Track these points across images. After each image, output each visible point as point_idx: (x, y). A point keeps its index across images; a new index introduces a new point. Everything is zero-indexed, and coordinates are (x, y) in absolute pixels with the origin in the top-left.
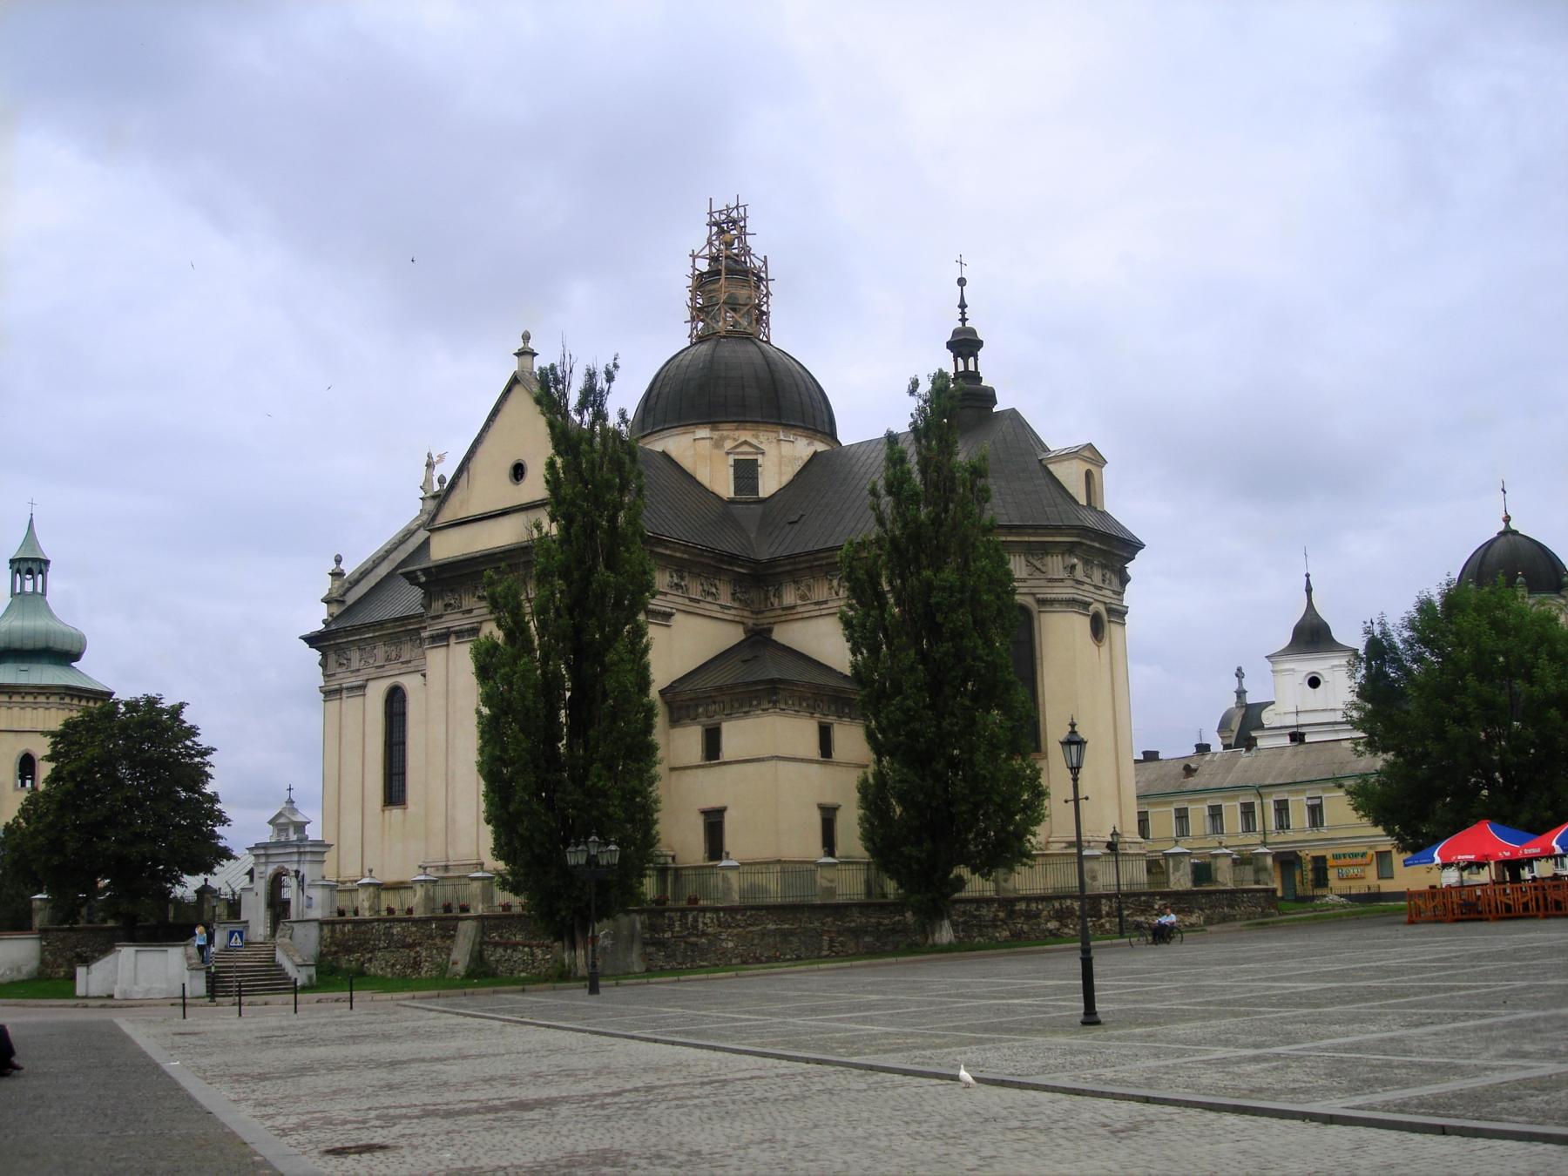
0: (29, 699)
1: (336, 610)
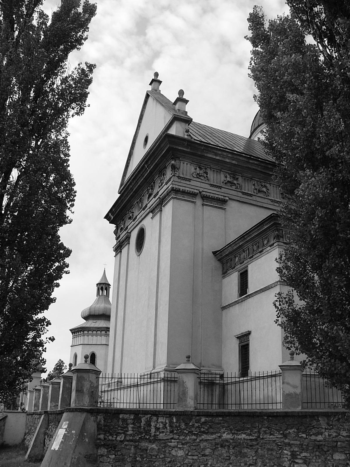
0: (94, 332)
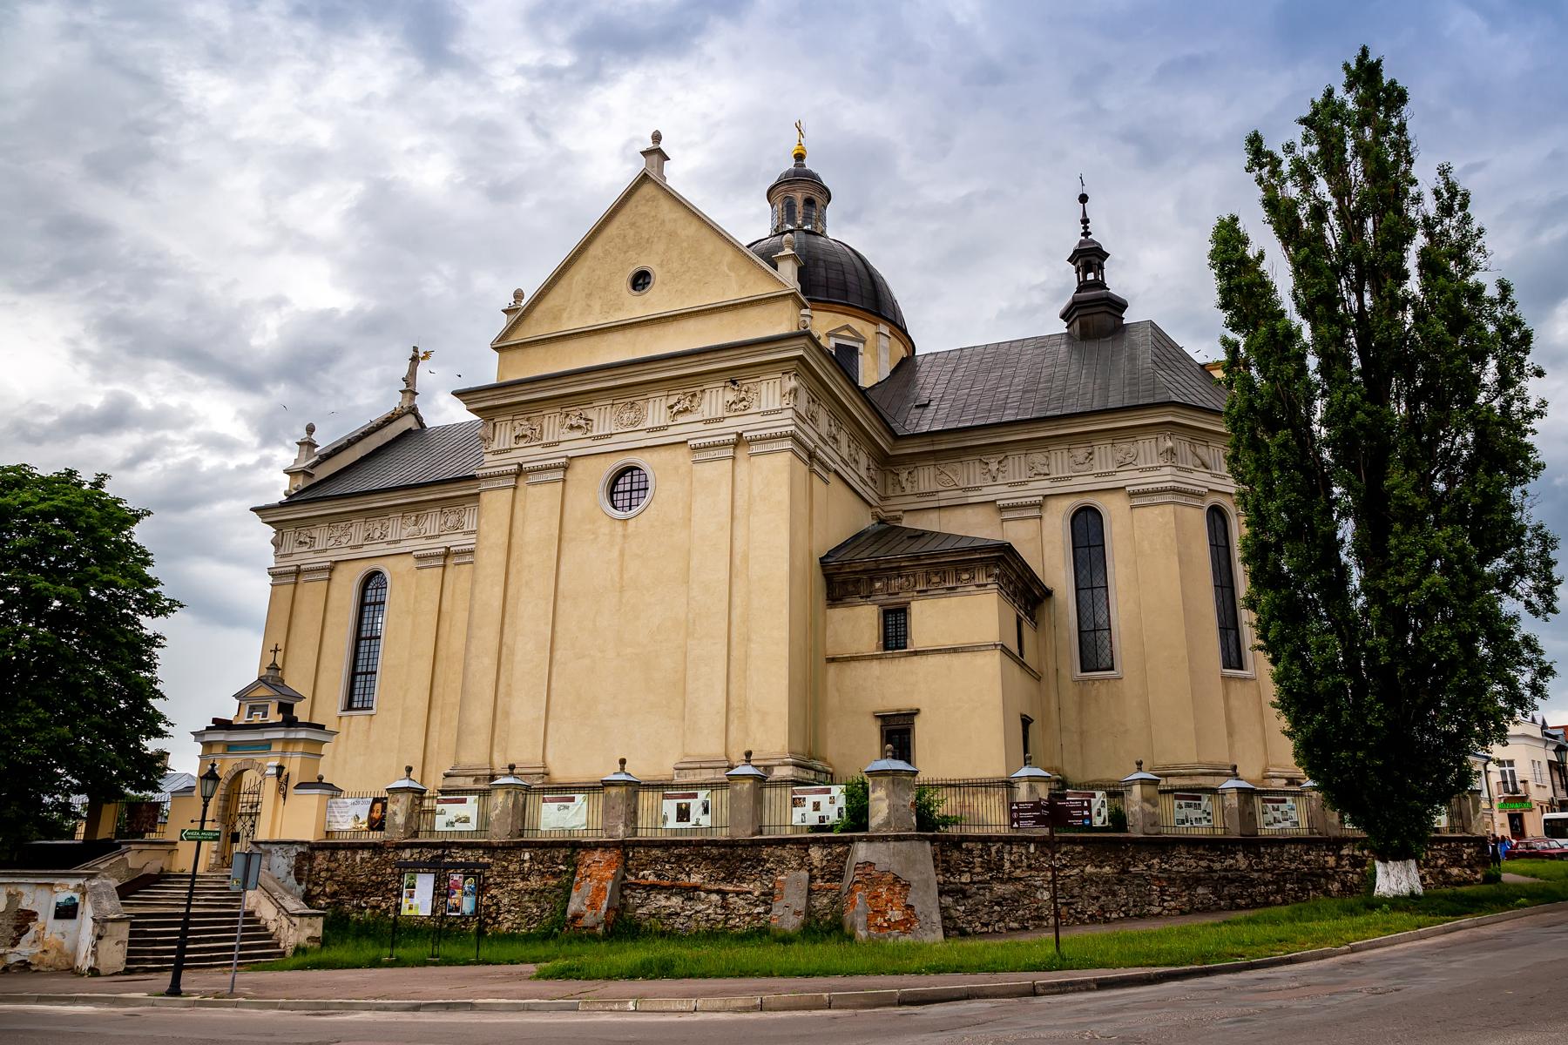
1: (301, 482)
